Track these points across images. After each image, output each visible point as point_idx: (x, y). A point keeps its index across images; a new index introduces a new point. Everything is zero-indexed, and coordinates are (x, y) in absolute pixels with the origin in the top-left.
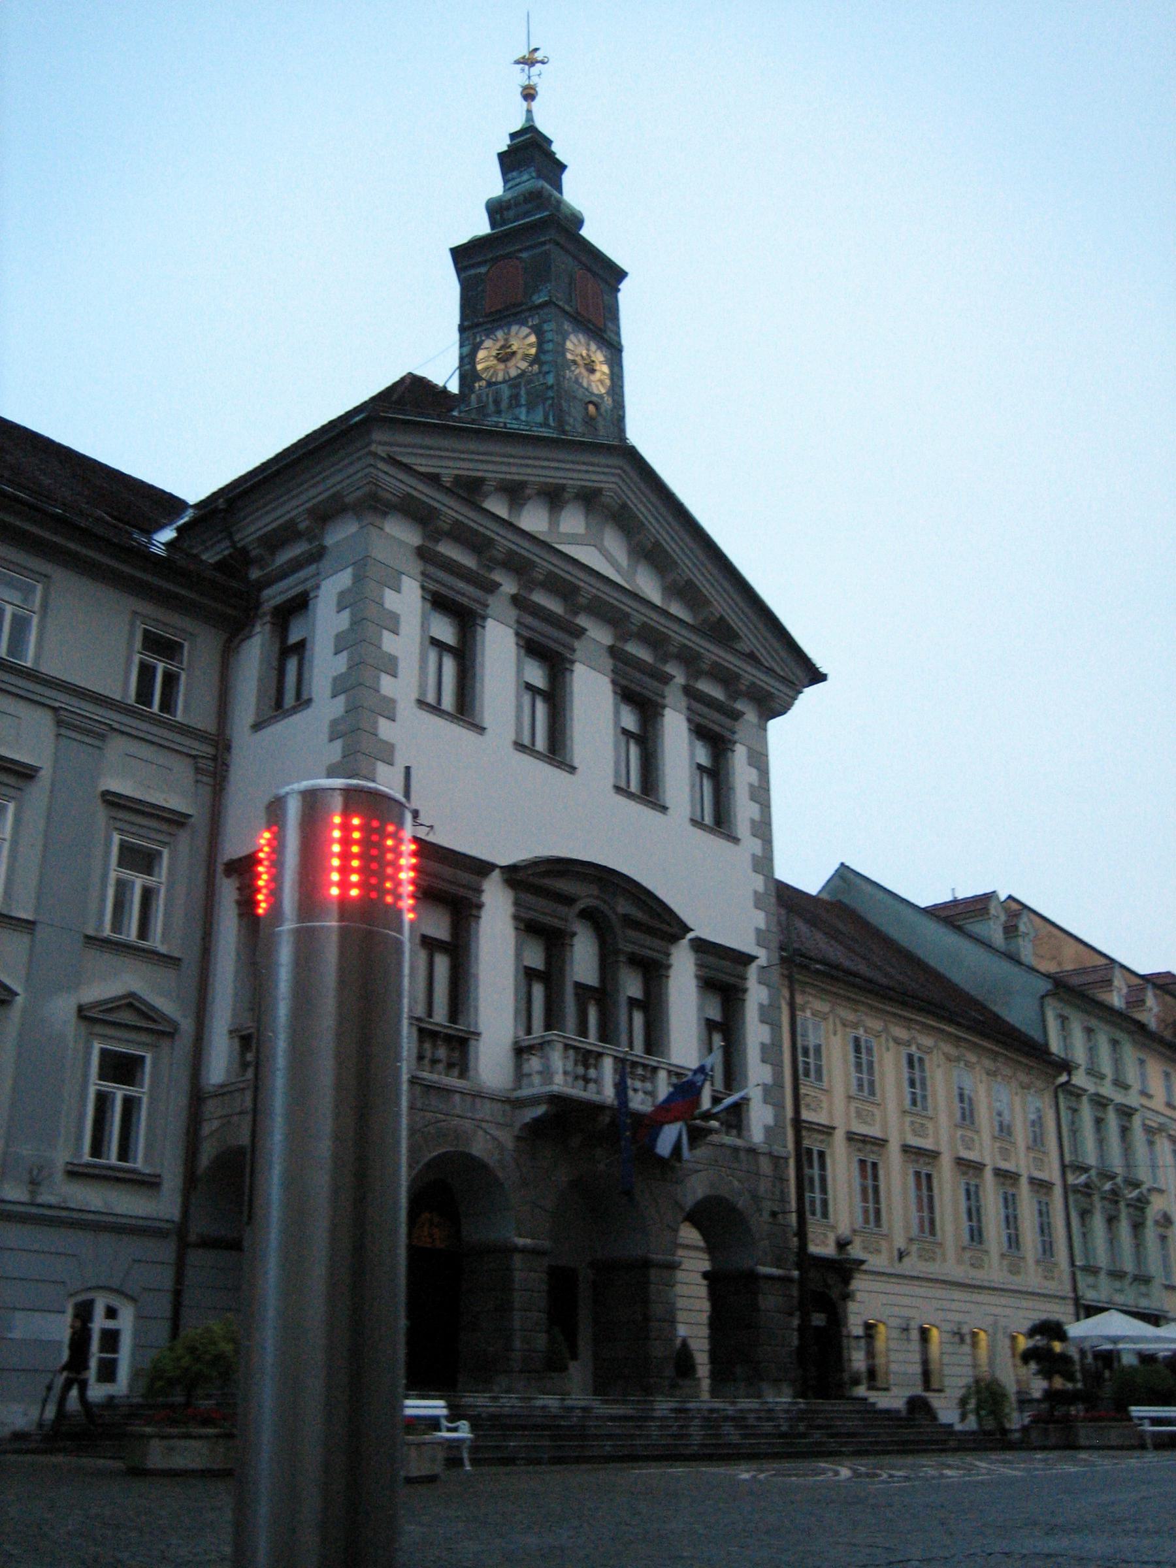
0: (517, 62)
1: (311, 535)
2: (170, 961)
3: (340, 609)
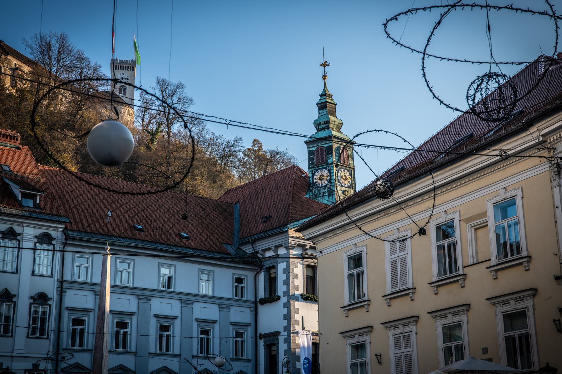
0: (321, 65)
1: (276, 251)
2: (249, 361)
3: (284, 273)
